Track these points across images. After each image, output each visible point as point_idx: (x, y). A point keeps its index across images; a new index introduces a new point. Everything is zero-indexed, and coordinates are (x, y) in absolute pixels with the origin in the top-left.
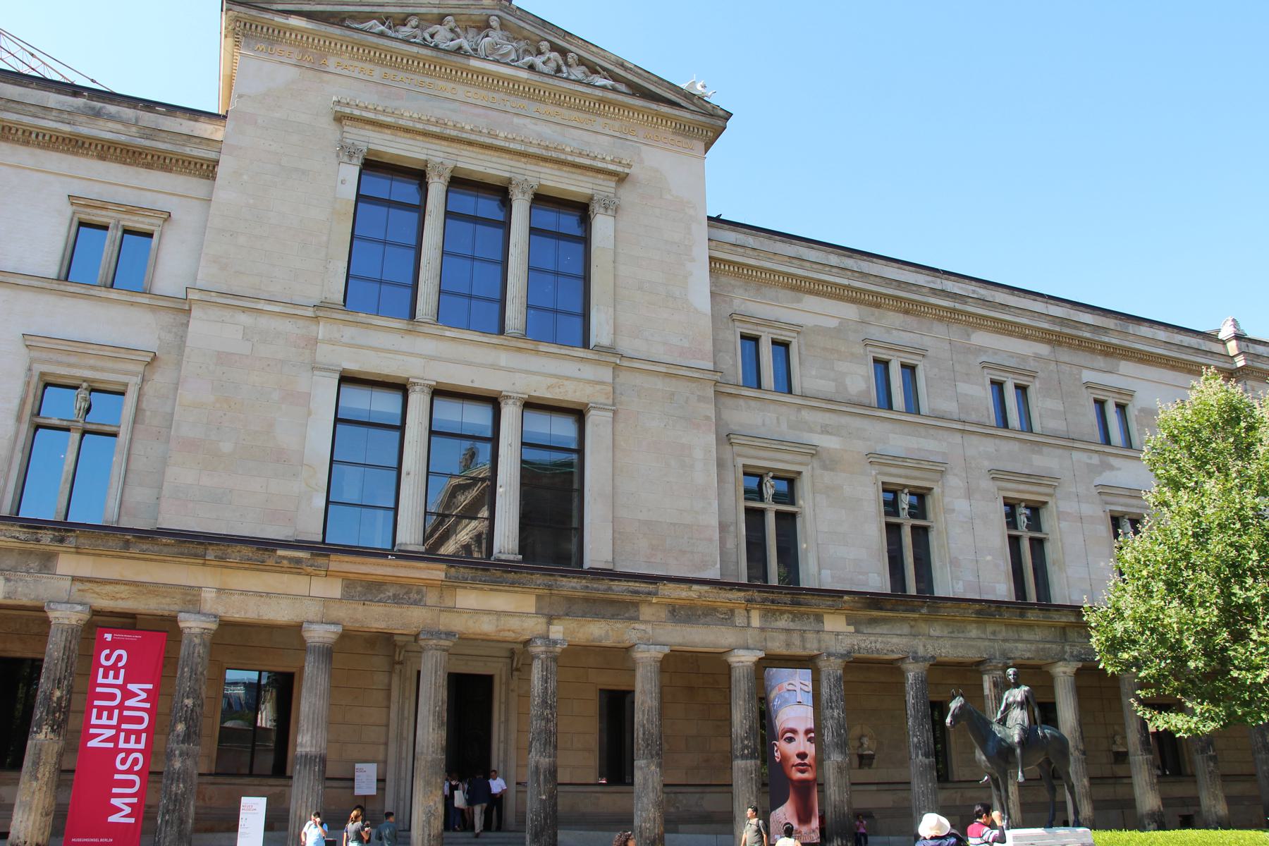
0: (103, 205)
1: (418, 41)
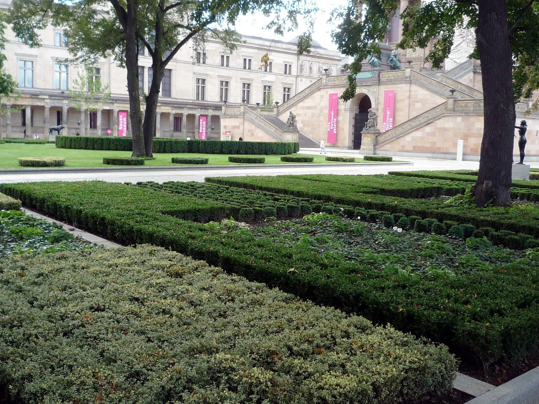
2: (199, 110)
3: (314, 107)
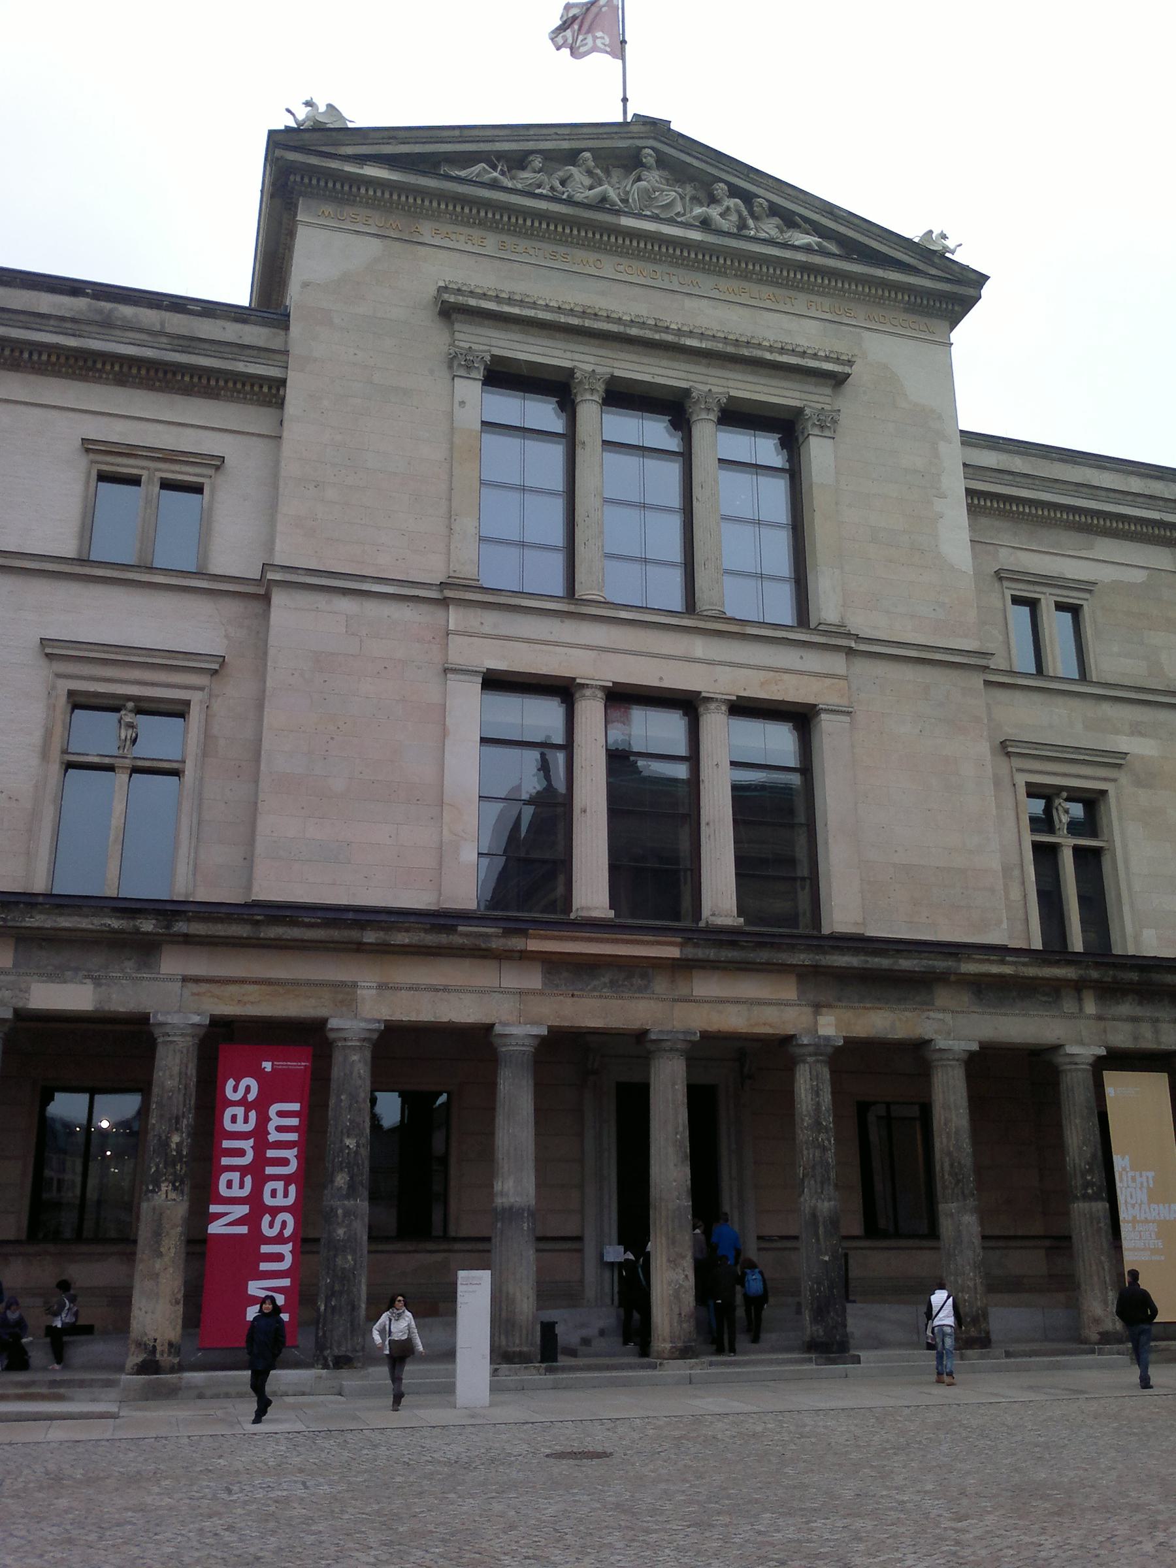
0: (131, 451)
1: (544, 192)
2: (1090, 1007)
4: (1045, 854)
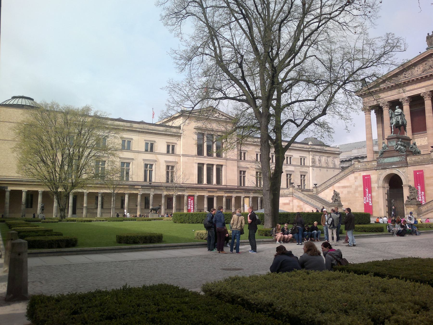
3: (349, 186)
4: (241, 176)
